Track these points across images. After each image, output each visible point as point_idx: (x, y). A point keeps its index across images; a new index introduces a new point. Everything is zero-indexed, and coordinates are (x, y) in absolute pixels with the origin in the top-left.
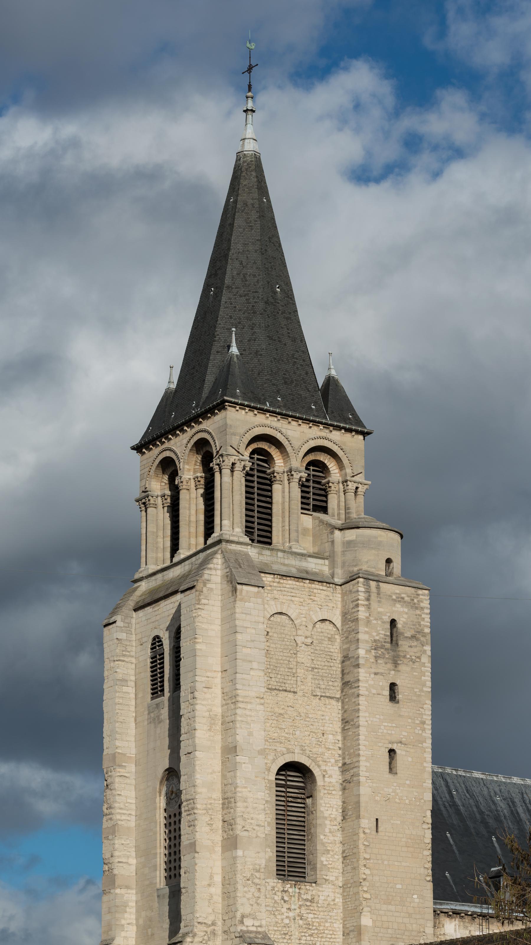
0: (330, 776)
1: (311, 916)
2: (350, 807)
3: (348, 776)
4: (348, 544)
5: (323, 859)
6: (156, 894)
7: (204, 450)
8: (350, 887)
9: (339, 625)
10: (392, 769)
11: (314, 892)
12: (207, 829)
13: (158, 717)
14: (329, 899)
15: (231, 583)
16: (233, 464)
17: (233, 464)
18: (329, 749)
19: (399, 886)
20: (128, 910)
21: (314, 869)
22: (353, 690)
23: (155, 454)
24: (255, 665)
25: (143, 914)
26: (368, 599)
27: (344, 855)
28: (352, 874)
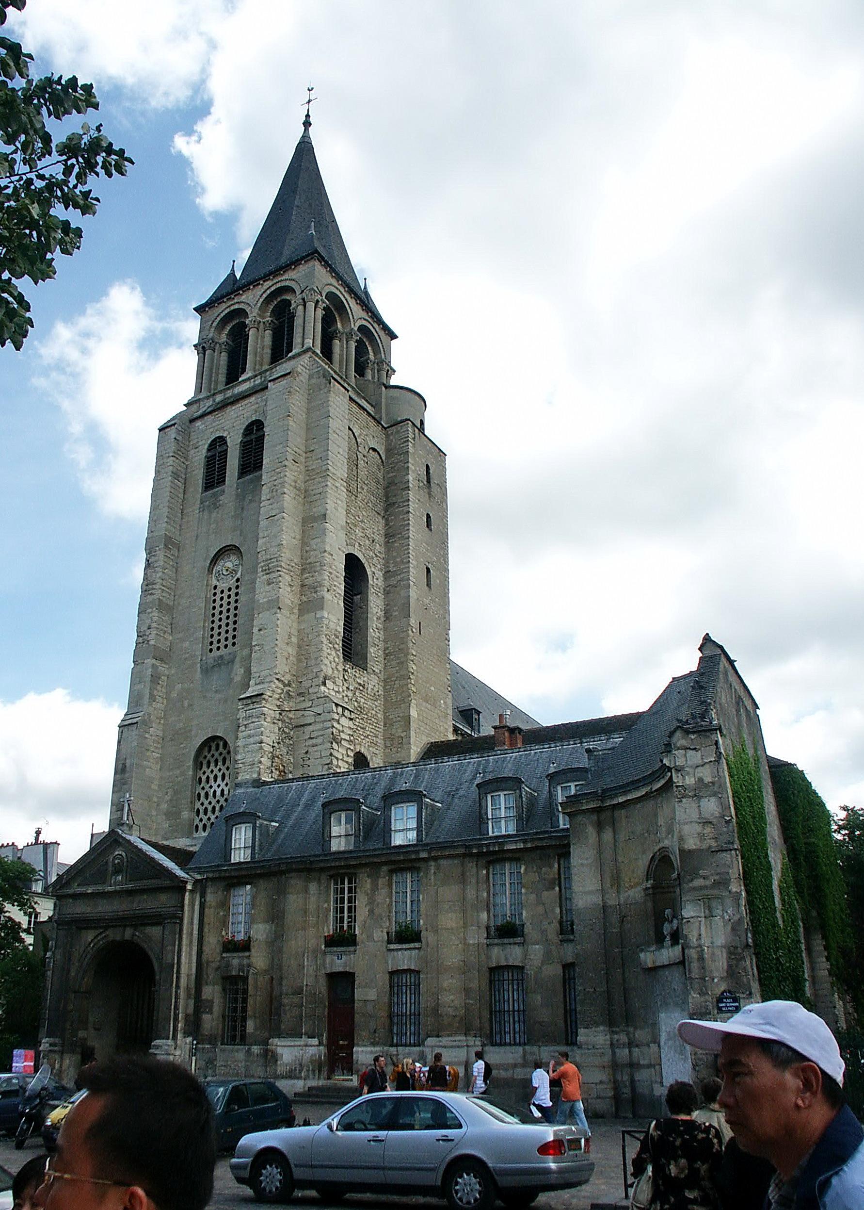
1: (363, 700)
4: (393, 398)
5: (372, 651)
7: (279, 299)
9: (384, 458)
10: (429, 585)
11: (365, 679)
12: (289, 589)
13: (215, 504)
14: (376, 690)
15: (324, 377)
16: (318, 301)
17: (318, 301)
18: (377, 556)
19: (432, 688)
21: (365, 659)
23: (223, 309)
26: (414, 439)
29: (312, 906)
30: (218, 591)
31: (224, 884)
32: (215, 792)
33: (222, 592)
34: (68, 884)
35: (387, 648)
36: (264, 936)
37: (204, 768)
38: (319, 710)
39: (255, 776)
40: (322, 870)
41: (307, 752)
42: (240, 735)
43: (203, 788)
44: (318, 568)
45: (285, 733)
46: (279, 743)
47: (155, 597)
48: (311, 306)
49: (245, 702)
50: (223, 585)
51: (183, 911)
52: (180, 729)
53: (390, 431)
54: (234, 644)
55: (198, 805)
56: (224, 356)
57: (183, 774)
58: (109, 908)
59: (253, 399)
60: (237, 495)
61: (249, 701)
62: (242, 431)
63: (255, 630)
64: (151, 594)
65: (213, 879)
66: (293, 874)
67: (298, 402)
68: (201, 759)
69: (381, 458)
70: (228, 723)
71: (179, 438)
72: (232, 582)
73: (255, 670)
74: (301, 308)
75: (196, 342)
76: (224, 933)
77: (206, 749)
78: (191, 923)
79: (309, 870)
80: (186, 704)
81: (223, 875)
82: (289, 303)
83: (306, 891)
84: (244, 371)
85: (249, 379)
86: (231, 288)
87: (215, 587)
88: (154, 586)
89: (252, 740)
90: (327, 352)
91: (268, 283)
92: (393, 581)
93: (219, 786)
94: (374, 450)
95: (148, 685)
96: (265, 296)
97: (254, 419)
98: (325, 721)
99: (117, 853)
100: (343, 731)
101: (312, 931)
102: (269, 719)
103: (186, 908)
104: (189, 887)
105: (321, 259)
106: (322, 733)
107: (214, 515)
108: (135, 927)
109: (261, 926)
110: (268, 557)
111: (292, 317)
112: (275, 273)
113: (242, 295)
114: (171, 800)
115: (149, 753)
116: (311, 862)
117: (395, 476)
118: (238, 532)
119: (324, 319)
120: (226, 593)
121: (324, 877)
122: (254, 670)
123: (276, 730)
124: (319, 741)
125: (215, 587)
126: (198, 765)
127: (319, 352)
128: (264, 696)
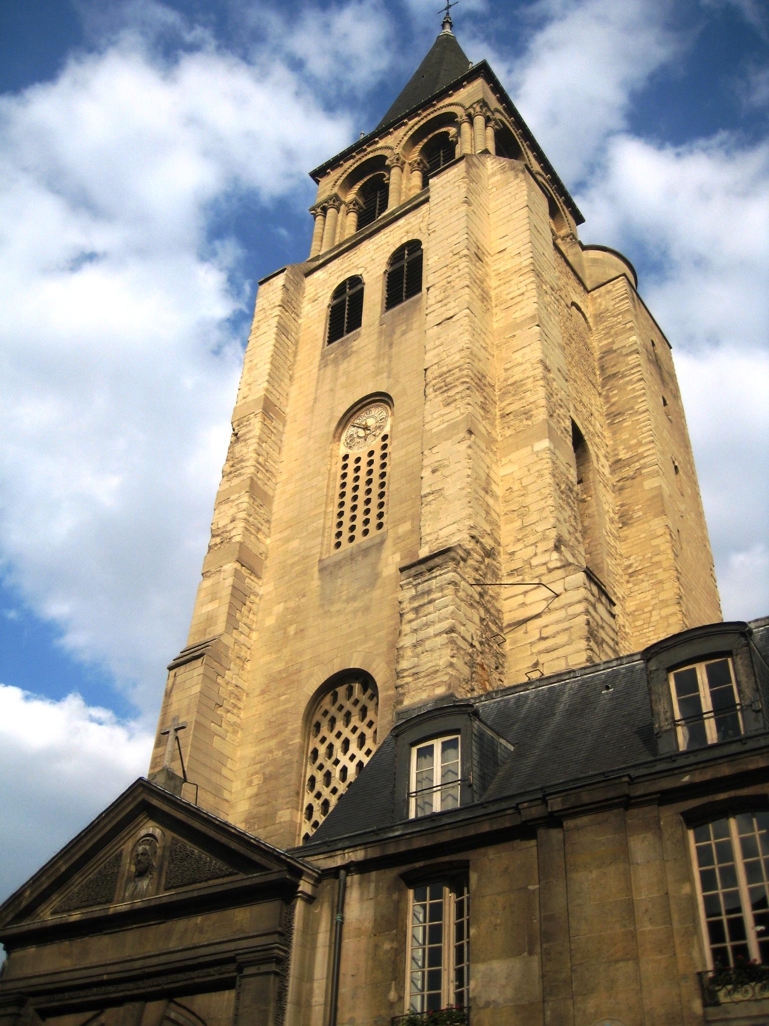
0: (603, 466)
2: (636, 508)
3: (627, 472)
4: (595, 261)
6: (316, 569)
7: (430, 136)
8: (651, 612)
9: (591, 324)
20: (248, 603)
22: (627, 379)
24: (546, 254)
25: (279, 608)
27: (630, 571)
28: (653, 592)
29: (645, 893)
30: (351, 462)
31: (391, 874)
32: (344, 770)
33: (358, 460)
34: (30, 910)
35: (630, 566)
36: (509, 992)
37: (324, 731)
38: (558, 588)
39: (440, 691)
40: (666, 798)
41: (536, 664)
42: (406, 628)
43: (321, 767)
44: (530, 386)
45: (491, 631)
46: (481, 643)
47: (245, 477)
48: (479, 121)
49: (413, 571)
50: (360, 451)
51: (288, 944)
52: (280, 672)
53: (595, 293)
54: (380, 526)
55: (309, 798)
56: (352, 218)
57: (283, 744)
58: (112, 955)
59: (401, 222)
60: (381, 333)
61: (423, 567)
62: (386, 260)
63: (426, 473)
64: (240, 475)
65: (361, 868)
66: (585, 820)
68: (318, 717)
69: (586, 319)
70: (371, 644)
71: (292, 289)
72: (375, 444)
73: (428, 530)
76: (392, 996)
77: (328, 698)
78: (307, 976)
79: (627, 803)
80: (292, 630)
81: (391, 850)
82: (447, 133)
83: (624, 854)
84: (384, 206)
87: (346, 457)
88: (244, 464)
89: (431, 631)
92: (627, 472)
93: (352, 757)
94: (579, 309)
95: (227, 599)
96: (410, 133)
97: (405, 240)
98: (570, 605)
99: (143, 832)
100: (603, 628)
101: (652, 964)
102: (461, 594)
103: (296, 938)
104: (305, 886)
106: (566, 625)
107: (344, 366)
108: (169, 995)
109: (499, 967)
110: (445, 369)
112: (427, 104)
113: (377, 143)
114: (257, 795)
115: (220, 711)
116: (632, 781)
117: (613, 343)
118: (385, 375)
120: (363, 464)
121: (669, 815)
122: (426, 530)
123: (477, 620)
124: (562, 639)
125: (346, 457)
126: (312, 726)
128: (452, 554)
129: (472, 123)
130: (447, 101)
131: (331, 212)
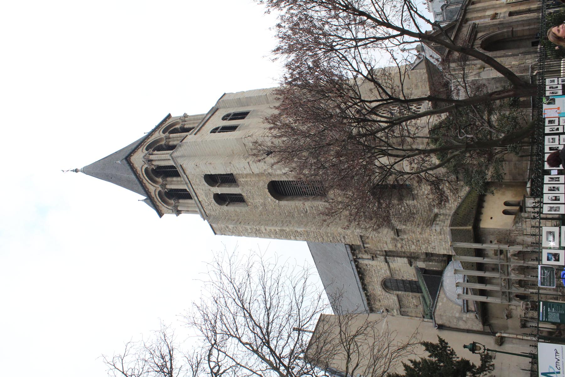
48: (152, 157)
67: (196, 160)
74: (154, 163)
75: (175, 215)
85: (188, 186)
86: (150, 200)
90: (172, 148)
91: (145, 181)
105: (130, 155)
111: (159, 167)
119: (158, 150)
127: (172, 151)
129: (152, 160)
130: (139, 169)
131: (179, 209)
